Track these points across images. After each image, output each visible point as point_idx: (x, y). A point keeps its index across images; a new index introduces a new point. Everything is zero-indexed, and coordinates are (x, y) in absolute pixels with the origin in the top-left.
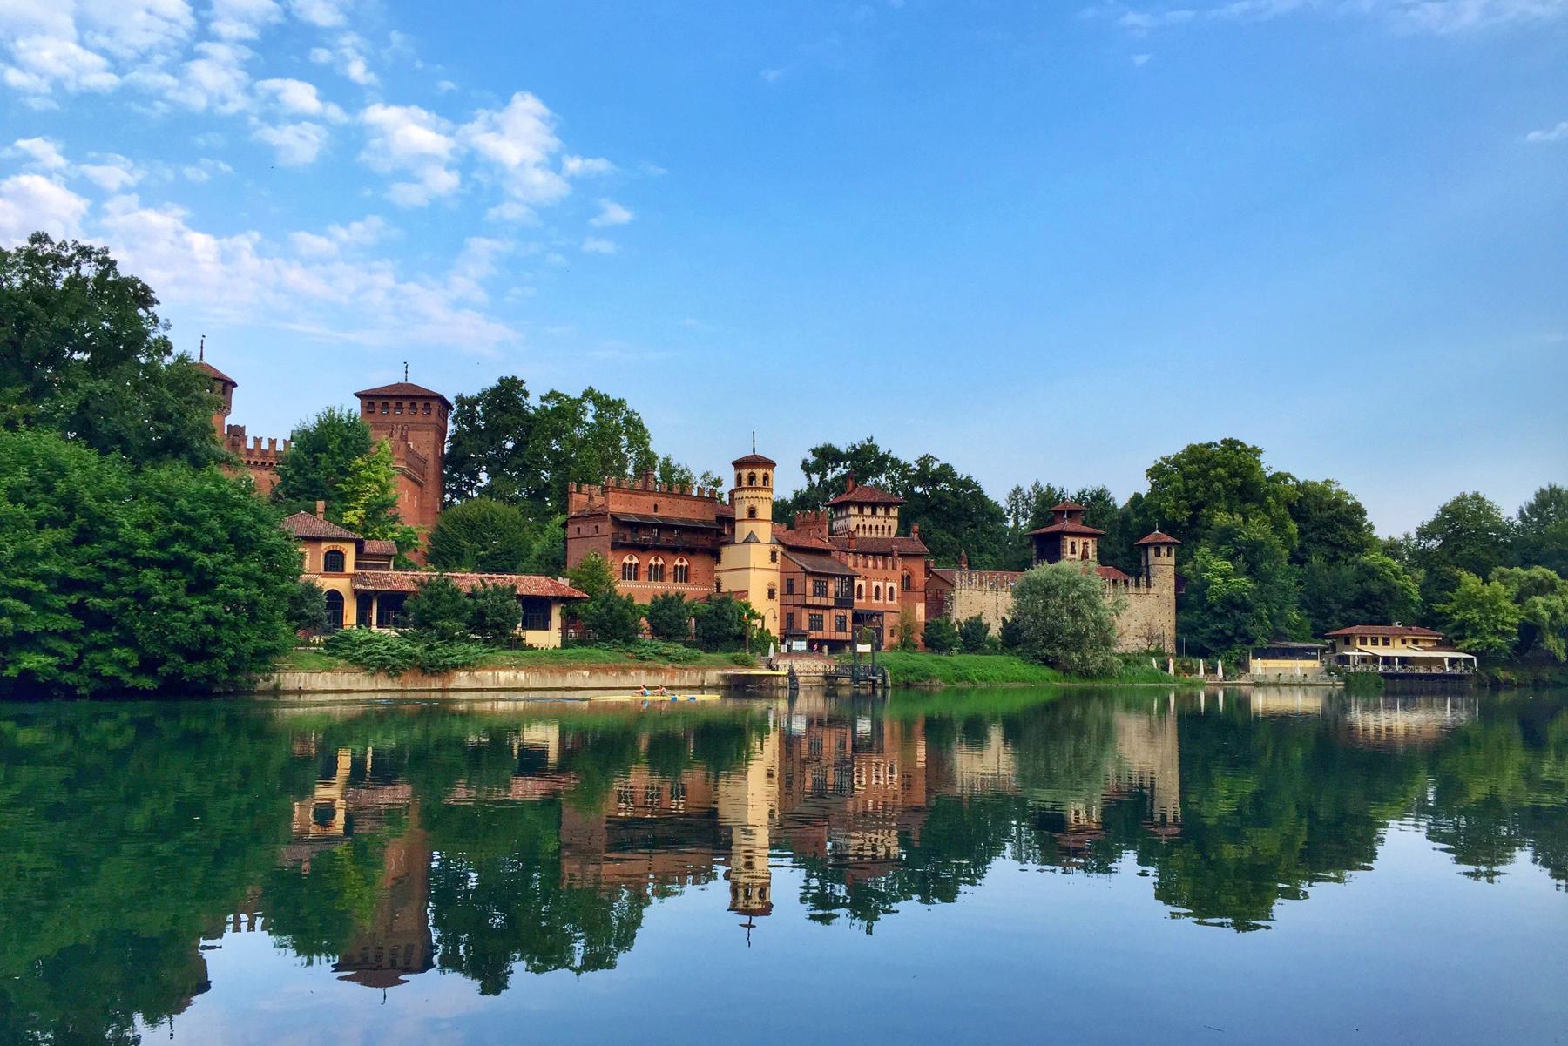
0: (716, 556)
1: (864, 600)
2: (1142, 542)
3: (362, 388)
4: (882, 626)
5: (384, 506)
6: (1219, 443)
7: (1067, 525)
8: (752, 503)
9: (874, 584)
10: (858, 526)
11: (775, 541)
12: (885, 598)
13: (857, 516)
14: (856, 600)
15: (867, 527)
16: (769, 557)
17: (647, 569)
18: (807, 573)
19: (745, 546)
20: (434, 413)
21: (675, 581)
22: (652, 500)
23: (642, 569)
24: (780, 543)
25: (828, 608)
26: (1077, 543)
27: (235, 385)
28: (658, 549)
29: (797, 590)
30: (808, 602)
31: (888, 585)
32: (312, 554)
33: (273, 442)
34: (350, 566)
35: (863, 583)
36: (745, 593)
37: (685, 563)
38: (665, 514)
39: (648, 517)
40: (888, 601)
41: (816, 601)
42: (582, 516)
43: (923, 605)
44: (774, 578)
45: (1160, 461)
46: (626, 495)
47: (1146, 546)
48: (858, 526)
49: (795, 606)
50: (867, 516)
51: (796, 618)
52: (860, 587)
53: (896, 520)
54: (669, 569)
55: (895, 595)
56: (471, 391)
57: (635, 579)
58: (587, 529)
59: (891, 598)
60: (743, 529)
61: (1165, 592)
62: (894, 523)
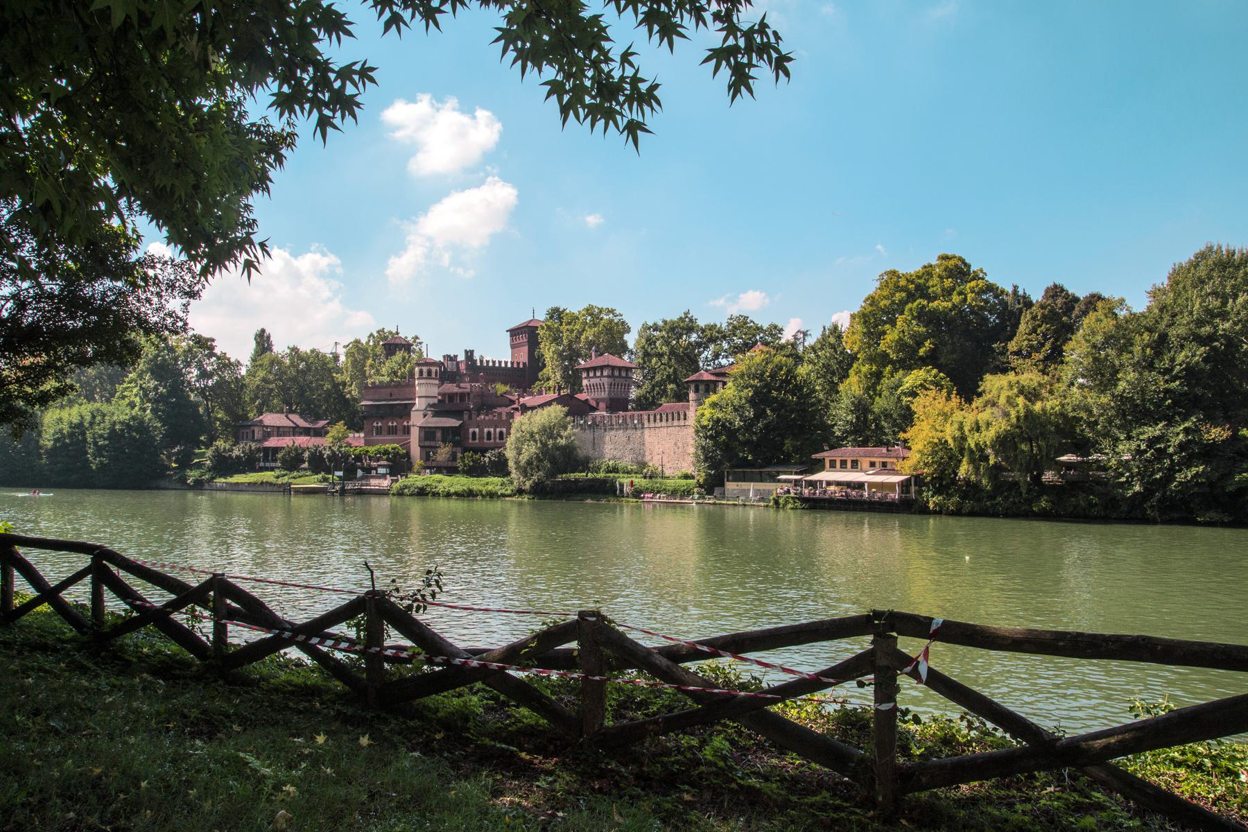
9: (486, 430)
12: (495, 438)
22: (388, 390)
31: (498, 430)
35: (477, 430)
41: (427, 443)
52: (474, 433)
54: (400, 427)
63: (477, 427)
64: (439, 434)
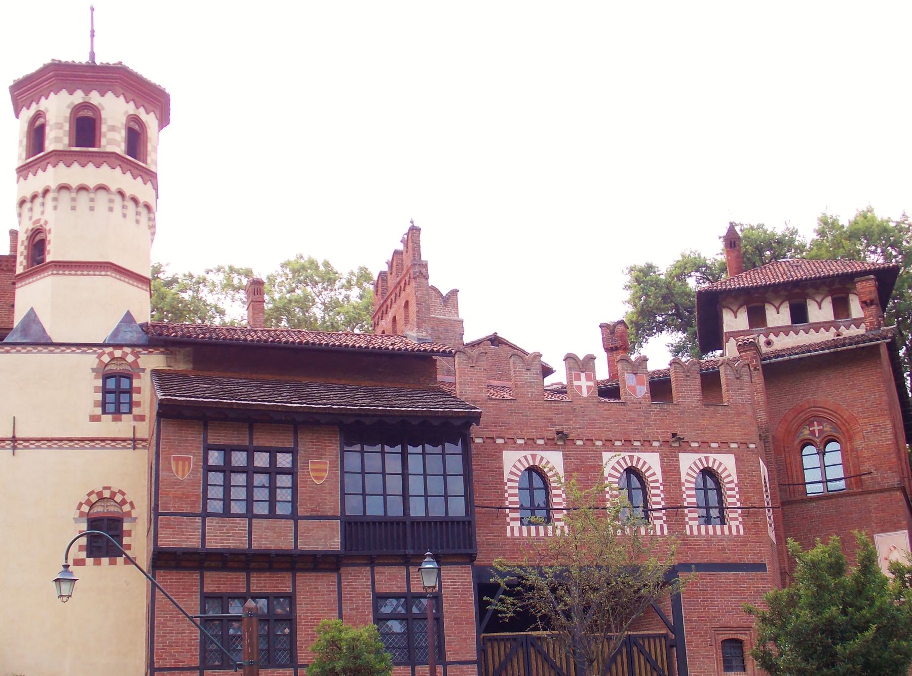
1: (561, 525)
4: (677, 628)
14: (514, 528)
31: (688, 463)
40: (693, 525)
50: (777, 331)
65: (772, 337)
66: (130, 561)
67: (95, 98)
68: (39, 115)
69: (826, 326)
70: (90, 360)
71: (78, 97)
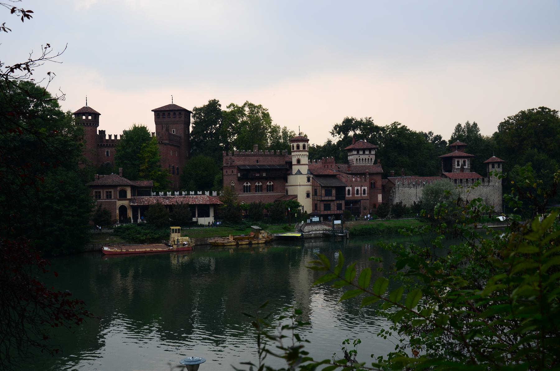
0: (286, 180)
1: (351, 196)
2: (486, 161)
3: (154, 109)
5: (155, 162)
6: (537, 108)
7: (456, 153)
8: (298, 157)
9: (356, 188)
10: (357, 159)
11: (309, 173)
12: (361, 194)
13: (356, 155)
14: (347, 196)
15: (361, 159)
16: (306, 180)
17: (254, 187)
18: (322, 186)
19: (296, 176)
20: (183, 117)
21: (268, 191)
22: (255, 158)
23: (252, 188)
24: (312, 174)
25: (333, 201)
26: (460, 161)
27: (100, 115)
28: (260, 179)
29: (318, 193)
30: (322, 199)
32: (114, 192)
33: (116, 136)
34: (129, 196)
35: (351, 188)
36: (296, 196)
37: (272, 183)
38: (261, 164)
39: (255, 165)
40: (363, 195)
41: (327, 198)
42: (227, 166)
43: (381, 195)
44: (309, 189)
45: (507, 119)
46: (244, 157)
47: (488, 163)
48: (357, 159)
49: (318, 200)
50: (361, 155)
51: (318, 206)
52: (349, 190)
53: (374, 156)
54: (265, 186)
55: (366, 192)
56: (200, 105)
57: (250, 192)
58: (229, 172)
59: (364, 193)
60: (295, 169)
61: (497, 184)
62: (373, 157)
63: (351, 186)
64: (334, 192)
65: (360, 155)
66: (310, 198)
67: (305, 143)
68: (298, 144)
69: (368, 154)
70: (306, 176)
71: (303, 143)
